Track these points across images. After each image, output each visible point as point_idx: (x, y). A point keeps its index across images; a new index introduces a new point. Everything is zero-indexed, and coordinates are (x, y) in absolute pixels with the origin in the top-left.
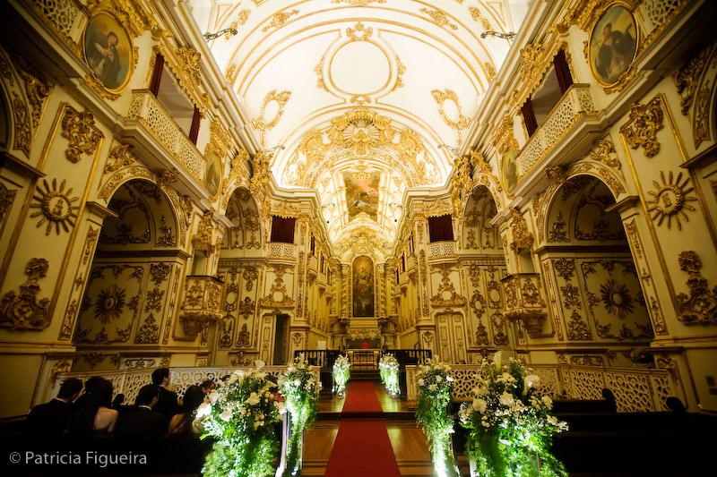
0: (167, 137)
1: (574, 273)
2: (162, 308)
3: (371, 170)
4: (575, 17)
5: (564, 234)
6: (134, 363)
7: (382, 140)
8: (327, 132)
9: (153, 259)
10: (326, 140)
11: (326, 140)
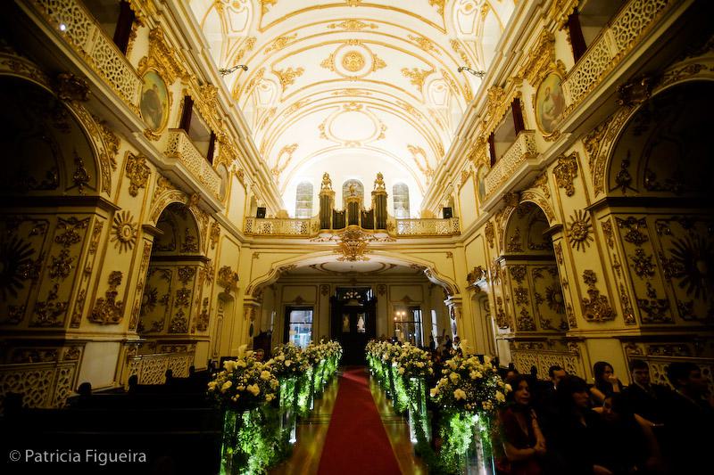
0: (191, 163)
1: (525, 277)
4: (526, 74)
5: (519, 245)
6: (168, 349)
9: (179, 263)
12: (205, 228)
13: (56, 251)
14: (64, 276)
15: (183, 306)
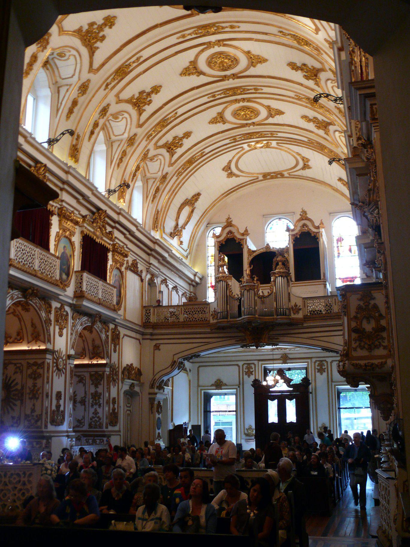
2: (102, 405)
12: (107, 337)
13: (30, 383)
14: (37, 399)
15: (97, 406)
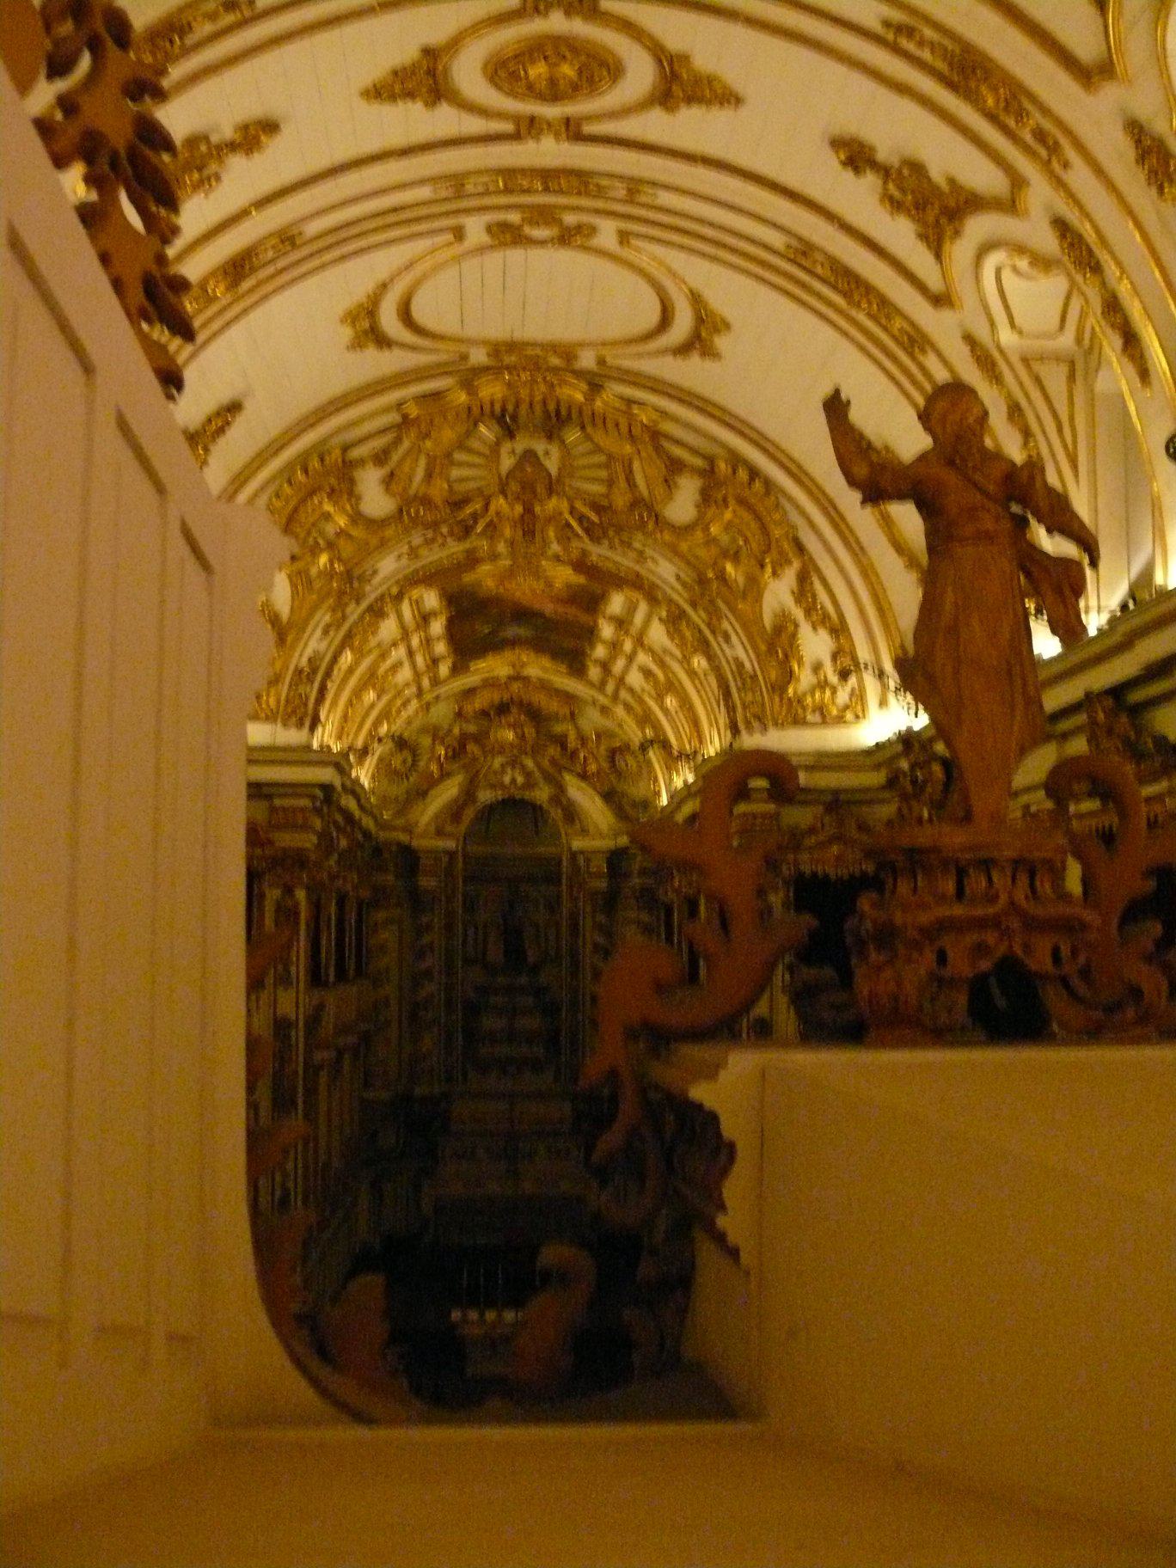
3: (563, 576)
7: (621, 500)
8: (380, 458)
10: (375, 499)
11: (375, 499)
